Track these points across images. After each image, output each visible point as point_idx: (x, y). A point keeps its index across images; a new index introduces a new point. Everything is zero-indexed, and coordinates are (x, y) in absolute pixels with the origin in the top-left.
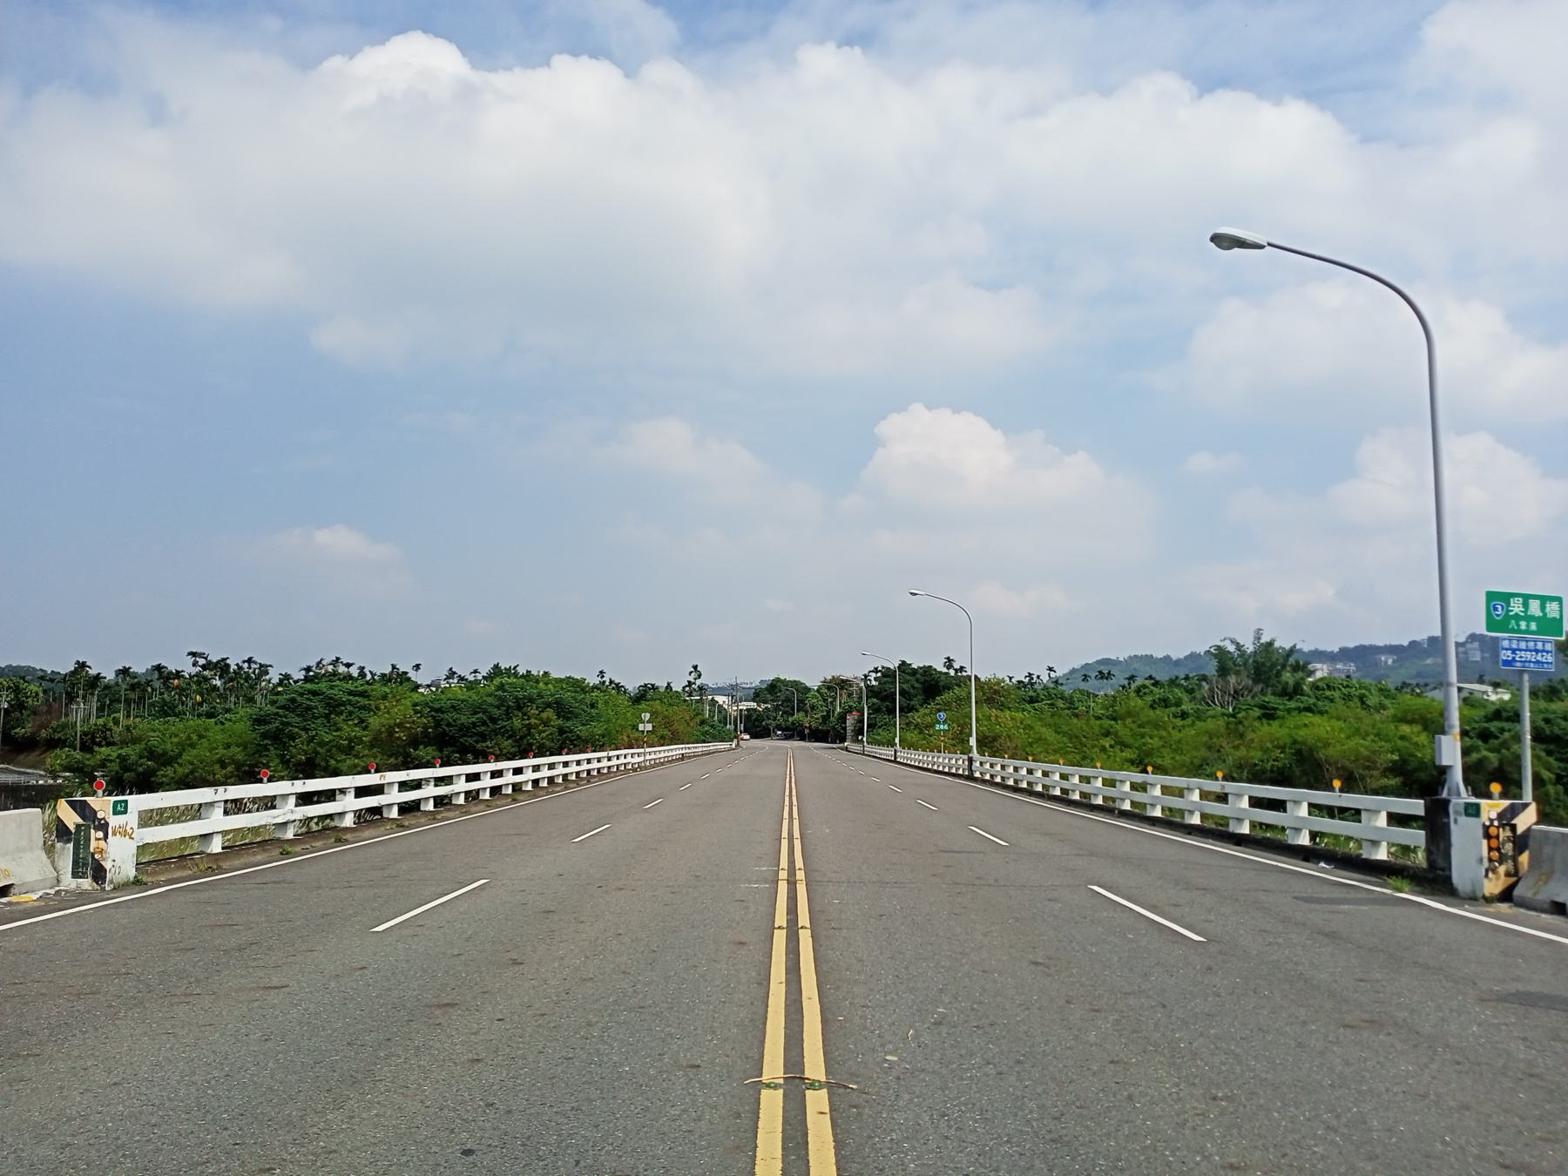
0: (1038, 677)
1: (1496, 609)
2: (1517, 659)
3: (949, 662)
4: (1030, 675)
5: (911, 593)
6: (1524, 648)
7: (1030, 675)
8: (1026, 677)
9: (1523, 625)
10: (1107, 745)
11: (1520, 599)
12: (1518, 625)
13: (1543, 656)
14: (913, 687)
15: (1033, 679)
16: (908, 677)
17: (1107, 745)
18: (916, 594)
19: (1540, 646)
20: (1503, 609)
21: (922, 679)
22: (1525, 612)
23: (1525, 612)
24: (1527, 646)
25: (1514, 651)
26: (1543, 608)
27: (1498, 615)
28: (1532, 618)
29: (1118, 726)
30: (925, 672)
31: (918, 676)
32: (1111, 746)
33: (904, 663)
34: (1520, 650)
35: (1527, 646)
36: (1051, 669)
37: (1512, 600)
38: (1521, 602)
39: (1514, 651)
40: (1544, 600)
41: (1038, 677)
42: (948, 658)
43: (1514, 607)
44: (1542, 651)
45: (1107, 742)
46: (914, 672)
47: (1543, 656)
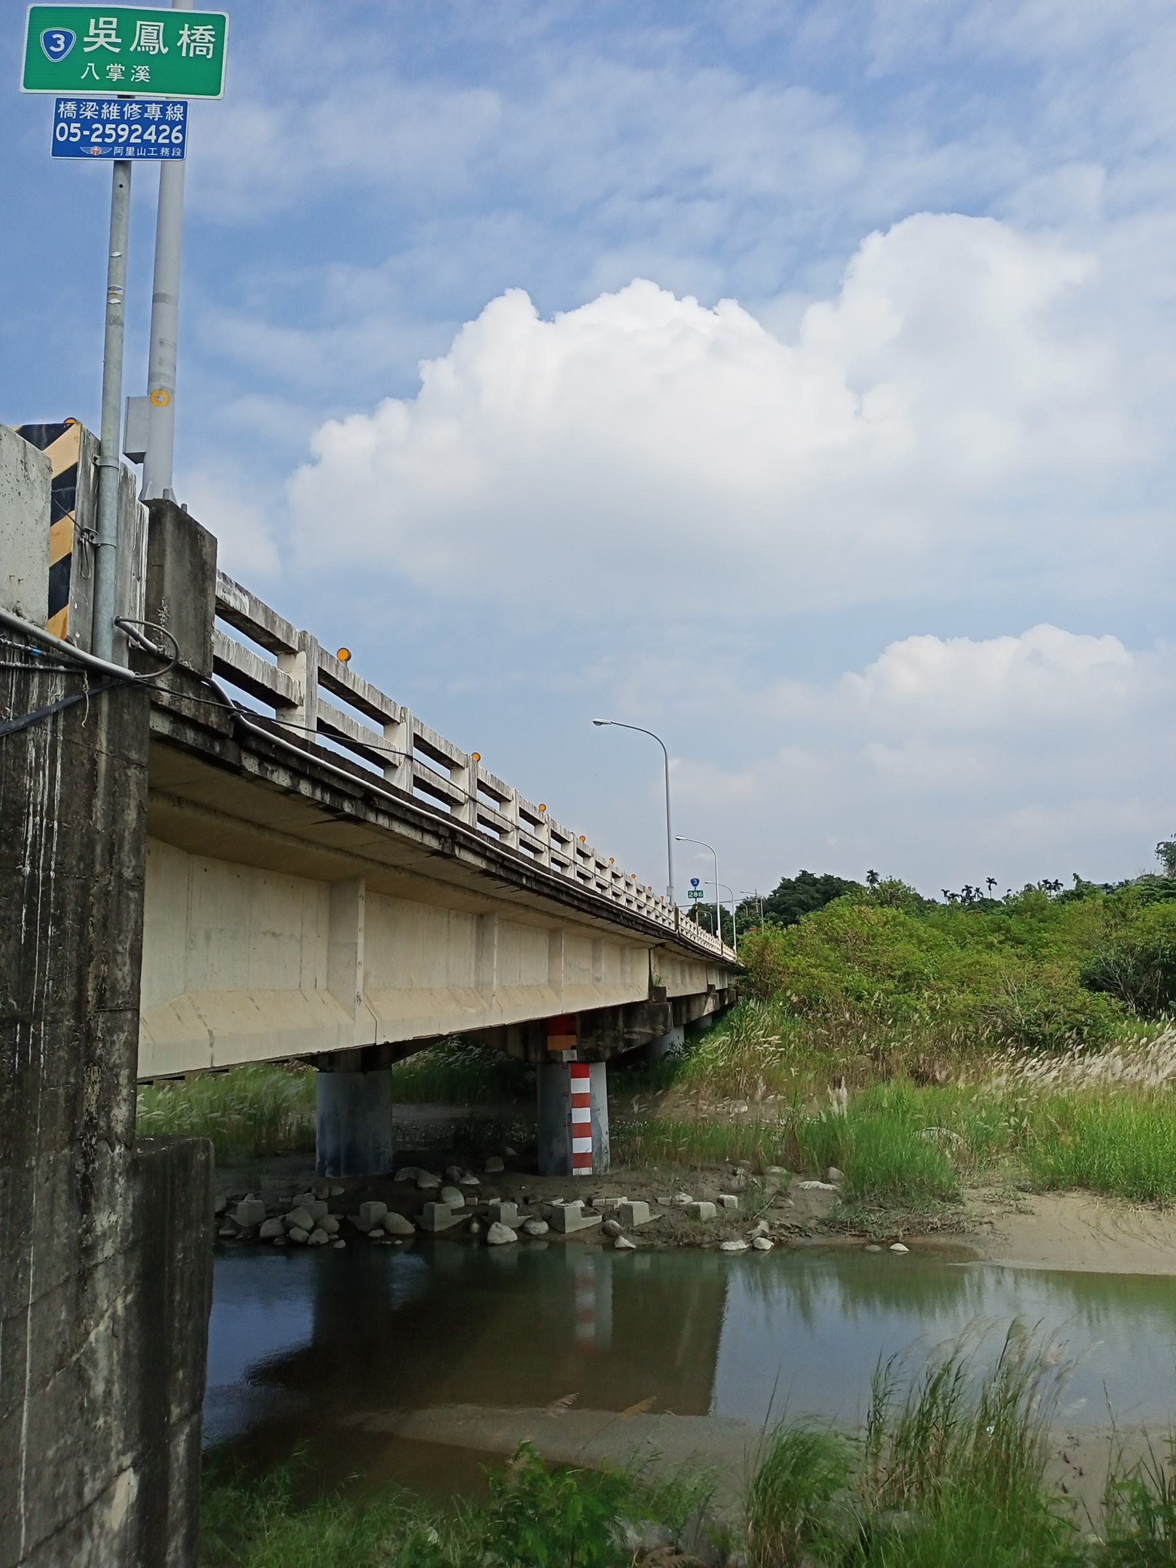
0: (977, 890)
1: (50, 41)
2: (93, 139)
3: (873, 877)
4: (968, 888)
5: (595, 722)
6: (115, 115)
7: (968, 888)
8: (963, 890)
9: (115, 72)
10: (996, 941)
11: (115, 20)
12: (103, 73)
13: (158, 133)
14: (813, 898)
15: (971, 892)
16: (808, 887)
17: (996, 941)
18: (602, 723)
19: (154, 112)
20: (67, 43)
21: (823, 889)
22: (124, 46)
23: (124, 46)
24: (122, 113)
25: (86, 124)
26: (171, 38)
27: (55, 55)
28: (144, 57)
29: (1013, 923)
30: (826, 881)
31: (818, 885)
32: (1001, 942)
33: (804, 873)
34: (104, 123)
35: (122, 113)
36: (991, 881)
37: (93, 21)
38: (114, 26)
39: (86, 124)
40: (173, 23)
41: (977, 890)
42: (871, 872)
43: (97, 35)
44: (162, 121)
45: (994, 939)
46: (816, 881)
47: (158, 133)
